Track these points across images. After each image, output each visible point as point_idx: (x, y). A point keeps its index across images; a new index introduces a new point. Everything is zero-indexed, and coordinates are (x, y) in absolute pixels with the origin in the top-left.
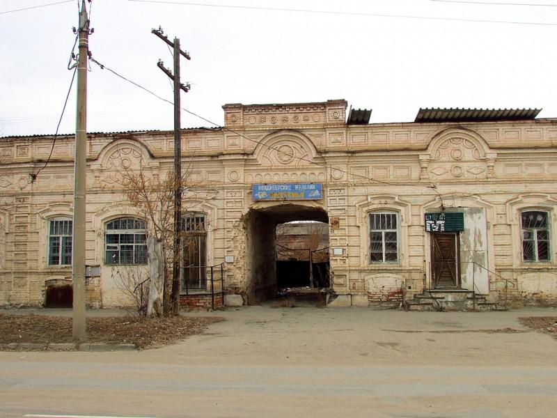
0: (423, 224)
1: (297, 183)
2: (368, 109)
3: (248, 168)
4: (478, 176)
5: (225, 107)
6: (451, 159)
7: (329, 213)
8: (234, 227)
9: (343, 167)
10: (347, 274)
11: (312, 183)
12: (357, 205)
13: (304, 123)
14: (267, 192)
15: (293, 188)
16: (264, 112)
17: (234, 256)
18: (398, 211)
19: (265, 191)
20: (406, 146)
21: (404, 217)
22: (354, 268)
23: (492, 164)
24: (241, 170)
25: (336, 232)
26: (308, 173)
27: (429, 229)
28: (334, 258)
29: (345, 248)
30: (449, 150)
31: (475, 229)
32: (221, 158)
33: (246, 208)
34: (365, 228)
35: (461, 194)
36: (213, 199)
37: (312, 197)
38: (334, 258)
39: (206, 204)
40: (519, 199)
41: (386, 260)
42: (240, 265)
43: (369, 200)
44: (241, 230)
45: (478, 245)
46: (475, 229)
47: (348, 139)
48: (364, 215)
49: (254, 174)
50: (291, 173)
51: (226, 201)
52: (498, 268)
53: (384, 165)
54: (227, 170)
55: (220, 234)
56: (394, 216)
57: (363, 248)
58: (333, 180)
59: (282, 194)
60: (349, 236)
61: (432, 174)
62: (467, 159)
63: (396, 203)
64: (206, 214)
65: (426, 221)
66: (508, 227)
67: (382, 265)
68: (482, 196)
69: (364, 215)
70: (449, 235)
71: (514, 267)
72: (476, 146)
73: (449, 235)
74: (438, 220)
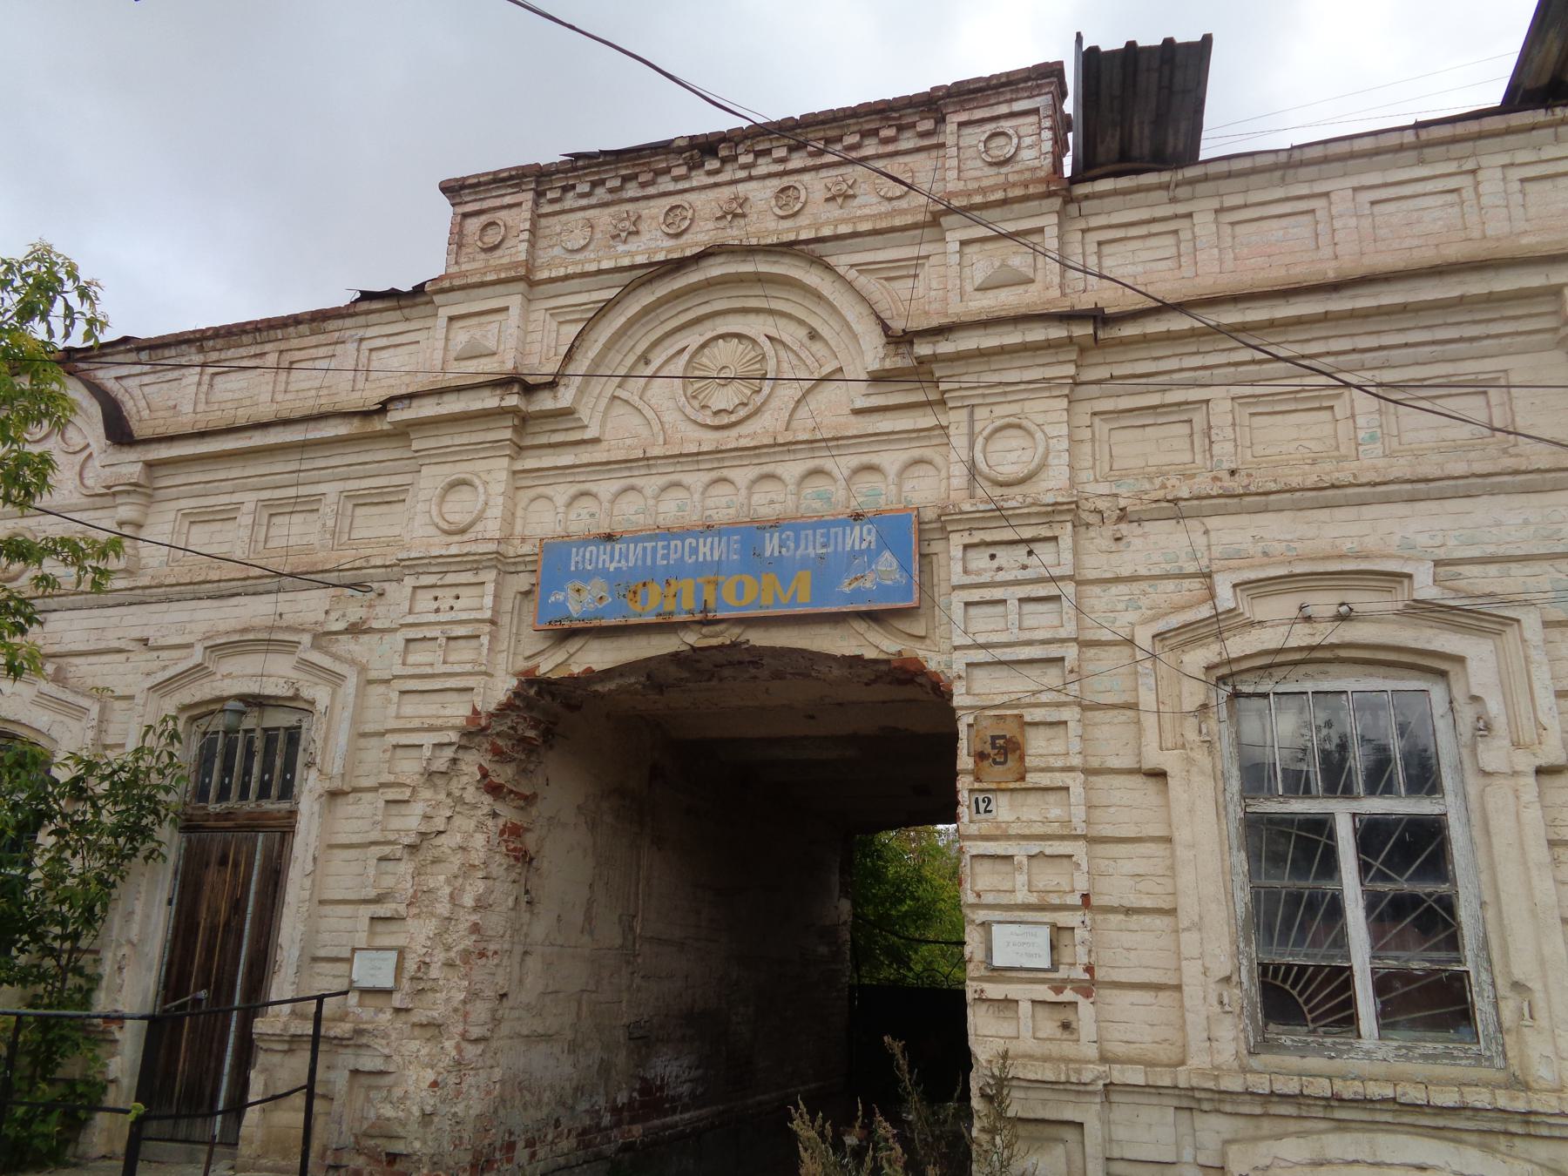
1: (776, 525)
2: (1186, 34)
3: (530, 463)
5: (452, 189)
7: (958, 689)
8: (430, 775)
9: (1048, 413)
10: (1088, 1113)
11: (857, 517)
12: (1143, 637)
13: (834, 211)
14: (614, 579)
15: (753, 557)
16: (632, 190)
17: (401, 952)
18: (1437, 667)
19: (604, 573)
20: (1454, 252)
21: (1494, 706)
22: (1136, 1076)
24: (495, 472)
25: (1004, 810)
26: (839, 466)
28: (994, 991)
29: (1063, 919)
32: (398, 415)
36: (356, 629)
37: (857, 594)
38: (994, 991)
39: (316, 657)
42: (434, 1008)
43: (1226, 597)
44: (471, 795)
48: (1194, 695)
49: (561, 492)
50: (753, 472)
51: (400, 637)
54: (432, 478)
55: (356, 819)
57: (1198, 926)
58: (984, 490)
59: (687, 586)
60: (1092, 840)
63: (1421, 610)
64: (308, 709)
67: (1352, 1063)
69: (1194, 695)
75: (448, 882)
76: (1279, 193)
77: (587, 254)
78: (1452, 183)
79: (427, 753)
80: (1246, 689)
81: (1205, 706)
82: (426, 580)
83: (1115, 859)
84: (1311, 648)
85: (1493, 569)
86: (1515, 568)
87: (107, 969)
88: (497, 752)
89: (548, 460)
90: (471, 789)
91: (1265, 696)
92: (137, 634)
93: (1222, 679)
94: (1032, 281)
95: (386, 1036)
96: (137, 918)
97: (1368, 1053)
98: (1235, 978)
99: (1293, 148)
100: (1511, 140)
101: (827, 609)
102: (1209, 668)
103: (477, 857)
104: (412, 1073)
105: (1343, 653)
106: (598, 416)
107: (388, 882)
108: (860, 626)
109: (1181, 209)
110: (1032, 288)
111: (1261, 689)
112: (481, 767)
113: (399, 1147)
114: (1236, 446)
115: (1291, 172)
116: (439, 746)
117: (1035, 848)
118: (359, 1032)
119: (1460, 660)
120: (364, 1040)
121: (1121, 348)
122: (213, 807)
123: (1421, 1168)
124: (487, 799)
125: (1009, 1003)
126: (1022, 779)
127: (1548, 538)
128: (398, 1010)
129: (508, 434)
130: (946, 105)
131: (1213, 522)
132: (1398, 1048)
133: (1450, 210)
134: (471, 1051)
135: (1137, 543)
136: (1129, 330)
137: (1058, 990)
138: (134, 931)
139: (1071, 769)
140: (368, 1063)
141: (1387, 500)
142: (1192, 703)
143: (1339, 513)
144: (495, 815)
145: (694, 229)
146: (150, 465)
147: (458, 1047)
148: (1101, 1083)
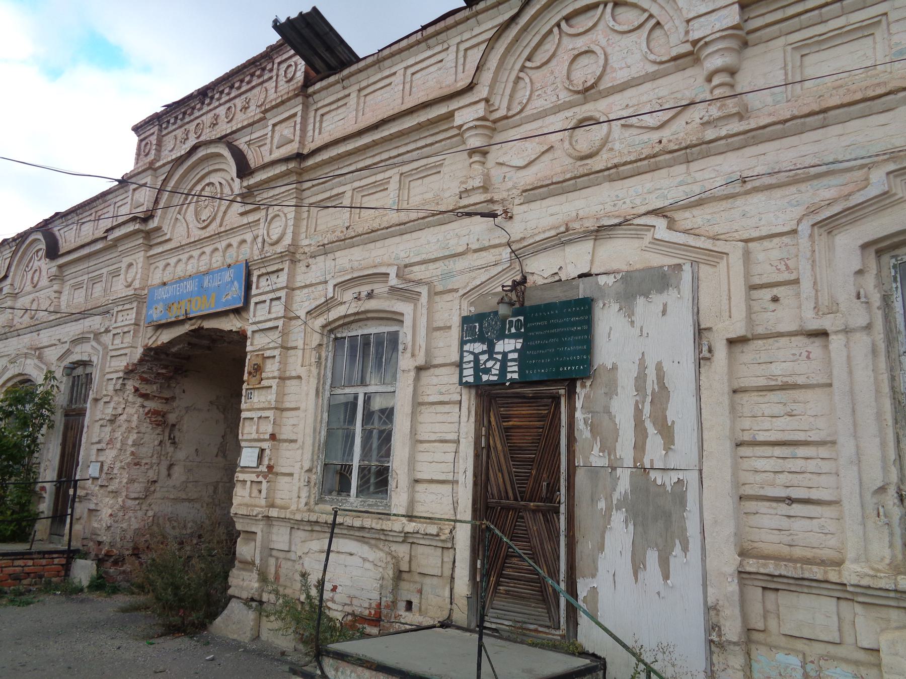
0: (455, 357)
3: (151, 253)
4: (665, 134)
5: (137, 129)
6: (564, 96)
7: (248, 343)
8: (116, 391)
23: (717, 62)
27: (469, 375)
29: (265, 445)
30: (560, 66)
31: (642, 366)
33: (139, 346)
34: (313, 382)
35: (591, 224)
40: (872, 191)
41: (360, 492)
44: (131, 398)
45: (654, 442)
46: (642, 366)
47: (310, 127)
49: (161, 264)
52: (752, 565)
53: (380, 177)
56: (394, 339)
61: (505, 169)
62: (621, 76)
65: (463, 343)
66: (815, 347)
68: (678, 216)
69: (316, 339)
70: (536, 397)
71: (851, 573)
72: (655, 10)
73: (535, 399)
74: (502, 336)
75: (122, 434)
76: (379, 76)
77: (174, 152)
78: (438, 58)
79: (114, 381)
80: (339, 335)
81: (320, 345)
82: (120, 308)
83: (288, 418)
84: (357, 313)
85: (423, 267)
86: (431, 266)
87: (42, 470)
88: (143, 380)
89: (159, 249)
90: (131, 396)
91: (345, 338)
92: (58, 338)
93: (331, 331)
94: (293, 141)
95: (97, 496)
96: (51, 450)
97: (352, 503)
98: (314, 470)
99: (379, 51)
100: (460, 28)
101: (220, 310)
102: (324, 327)
103: (134, 425)
104: (104, 511)
105: (369, 315)
106: (170, 228)
107: (103, 435)
108: (232, 316)
109: (346, 92)
110: (294, 143)
111: (344, 335)
112: (134, 387)
113: (99, 539)
114: (351, 214)
115: (381, 64)
116: (118, 378)
117: (259, 414)
118: (87, 494)
119: (402, 314)
120: (89, 497)
121: (313, 171)
122: (73, 407)
123: (351, 554)
124: (139, 400)
125: (244, 481)
126: (260, 383)
127: (444, 248)
128: (101, 486)
129: (141, 241)
130: (273, 55)
131: (338, 254)
132: (361, 502)
133: (439, 72)
134: (130, 503)
135: (313, 267)
136: (310, 162)
137: (258, 476)
138: (50, 455)
139: (274, 378)
140: (92, 507)
141: (393, 236)
142: (315, 343)
143: (379, 244)
144: (143, 407)
145: (204, 133)
146: (60, 267)
147: (123, 501)
148: (260, 516)
